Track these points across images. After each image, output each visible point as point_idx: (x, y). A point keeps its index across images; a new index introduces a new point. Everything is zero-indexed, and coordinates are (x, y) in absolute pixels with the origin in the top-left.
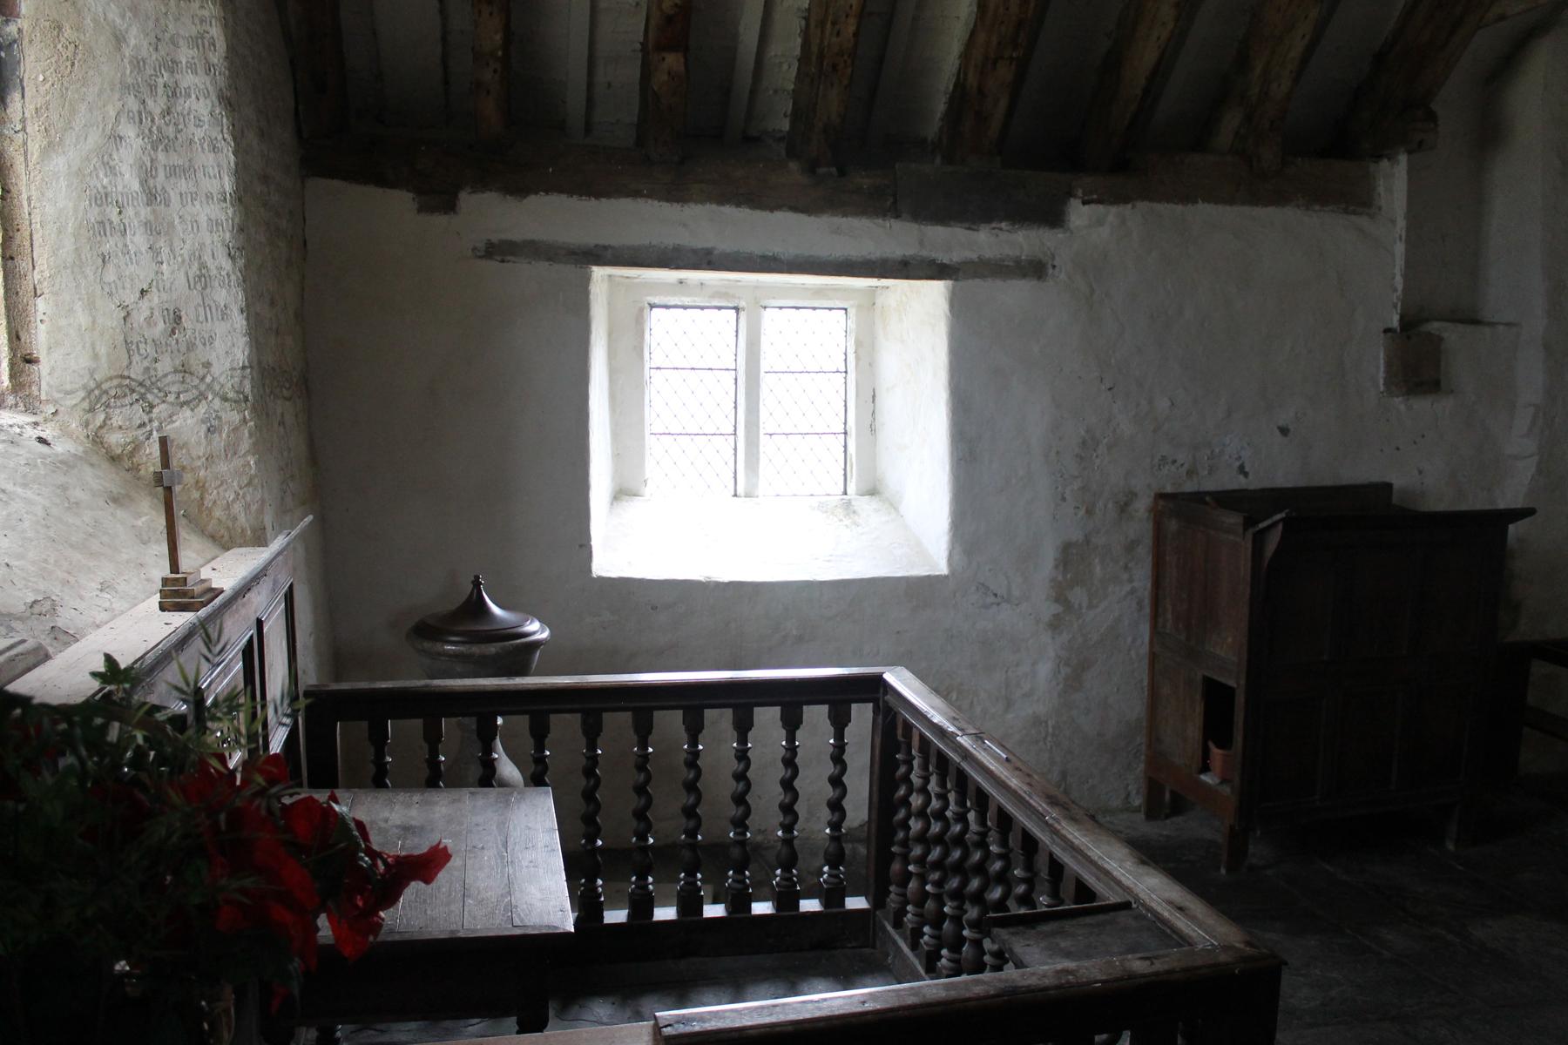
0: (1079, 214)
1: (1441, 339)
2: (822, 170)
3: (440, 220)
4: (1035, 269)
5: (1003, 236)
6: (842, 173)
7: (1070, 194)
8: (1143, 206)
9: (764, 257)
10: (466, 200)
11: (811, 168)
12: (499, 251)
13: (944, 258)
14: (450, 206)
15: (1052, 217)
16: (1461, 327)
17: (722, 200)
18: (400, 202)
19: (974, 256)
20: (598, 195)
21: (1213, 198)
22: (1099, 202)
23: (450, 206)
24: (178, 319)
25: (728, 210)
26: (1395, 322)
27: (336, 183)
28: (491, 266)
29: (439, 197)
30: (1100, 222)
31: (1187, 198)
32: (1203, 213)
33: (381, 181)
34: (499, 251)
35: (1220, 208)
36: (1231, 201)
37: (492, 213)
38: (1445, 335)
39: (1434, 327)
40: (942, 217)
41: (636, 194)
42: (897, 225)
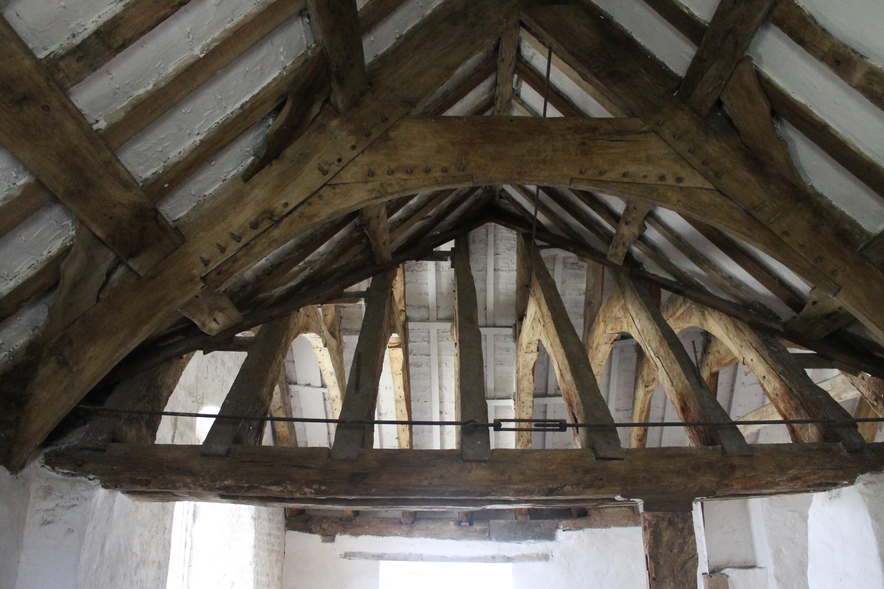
0: (561, 534)
1: (727, 576)
2: (463, 524)
3: (329, 545)
4: (545, 557)
5: (532, 545)
6: (471, 524)
7: (557, 528)
8: (587, 530)
9: (442, 557)
10: (338, 537)
11: (459, 523)
12: (348, 555)
13: (508, 555)
14: (333, 540)
15: (551, 537)
16: (737, 571)
17: (426, 536)
18: (316, 538)
19: (520, 553)
20: (383, 535)
21: (617, 524)
22: (570, 530)
23: (333, 540)
24: (233, 583)
25: (428, 540)
26: (707, 571)
27: (296, 532)
28: (346, 560)
29: (329, 537)
30: (570, 538)
31: (607, 526)
32: (614, 531)
33: (310, 531)
34: (348, 555)
35: (621, 528)
36: (626, 525)
37: (345, 542)
38: (730, 575)
39: (726, 571)
40: (507, 539)
41: (396, 535)
42: (489, 543)
